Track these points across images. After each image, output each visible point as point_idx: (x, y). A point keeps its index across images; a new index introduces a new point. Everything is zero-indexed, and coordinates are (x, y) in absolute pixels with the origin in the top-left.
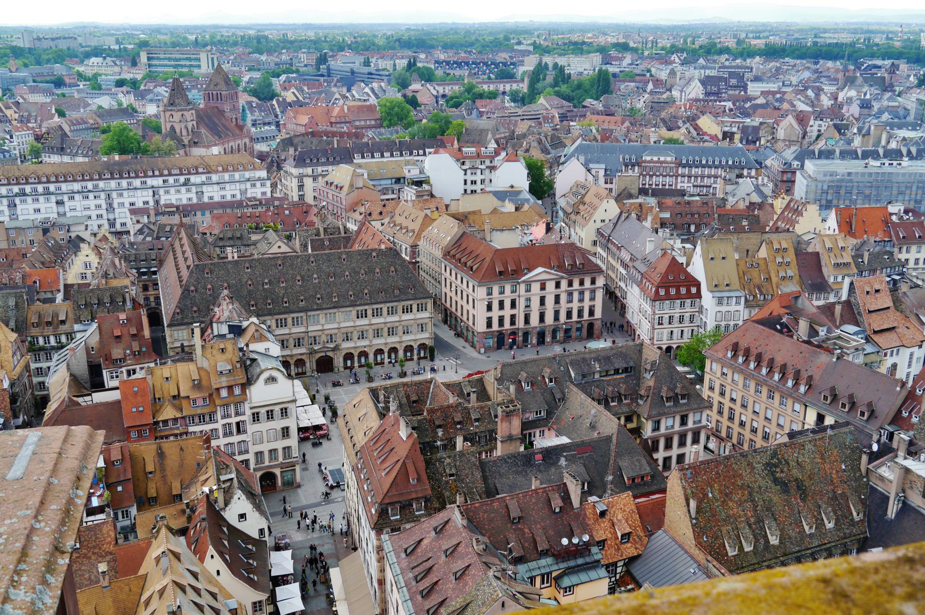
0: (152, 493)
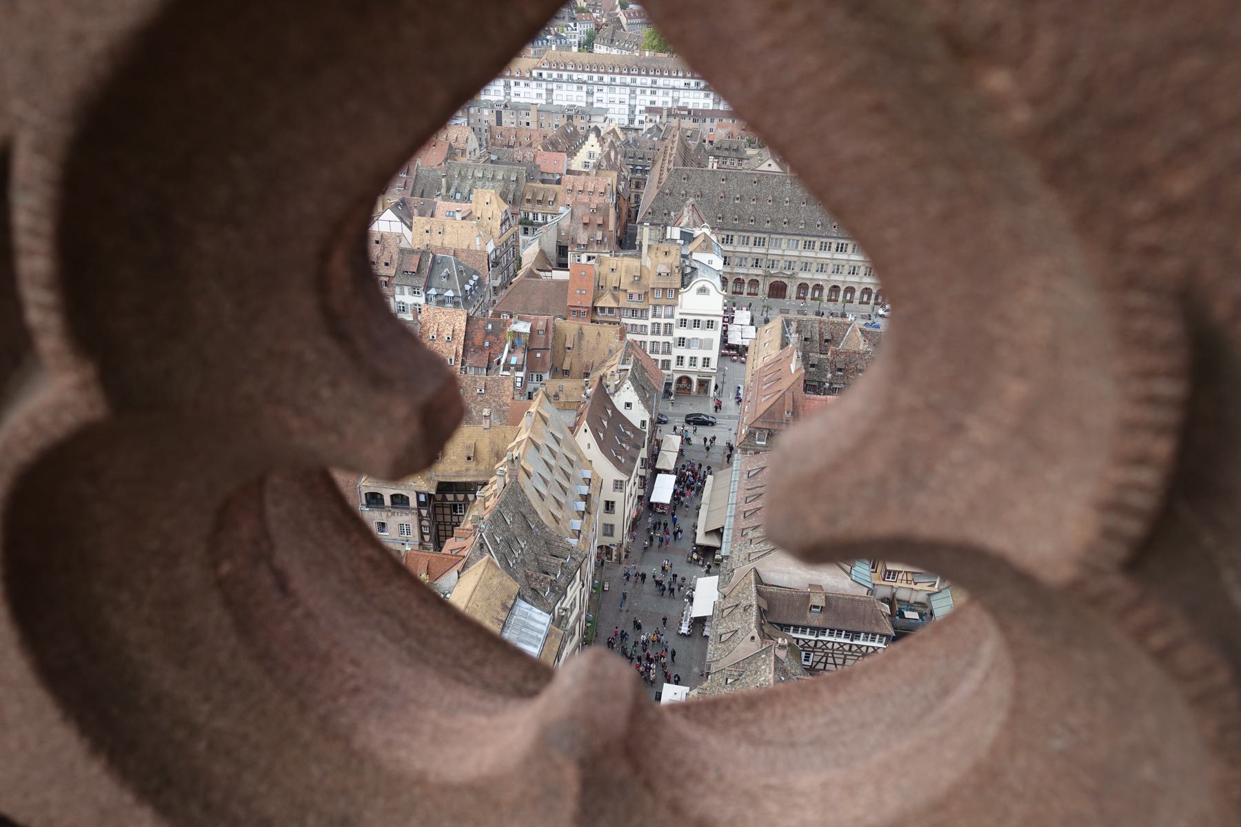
0: (566, 367)
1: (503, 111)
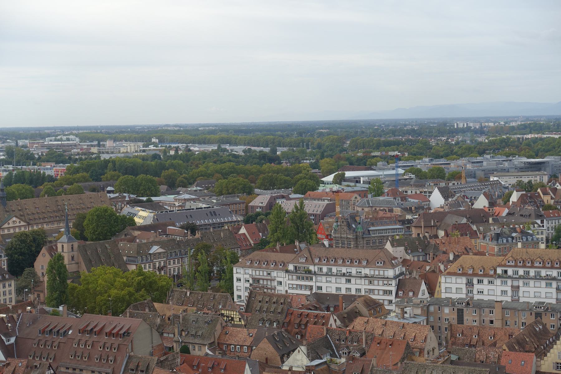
1: (465, 309)
